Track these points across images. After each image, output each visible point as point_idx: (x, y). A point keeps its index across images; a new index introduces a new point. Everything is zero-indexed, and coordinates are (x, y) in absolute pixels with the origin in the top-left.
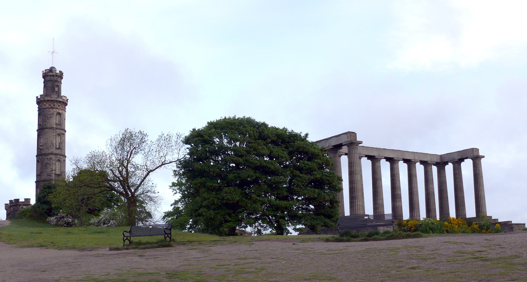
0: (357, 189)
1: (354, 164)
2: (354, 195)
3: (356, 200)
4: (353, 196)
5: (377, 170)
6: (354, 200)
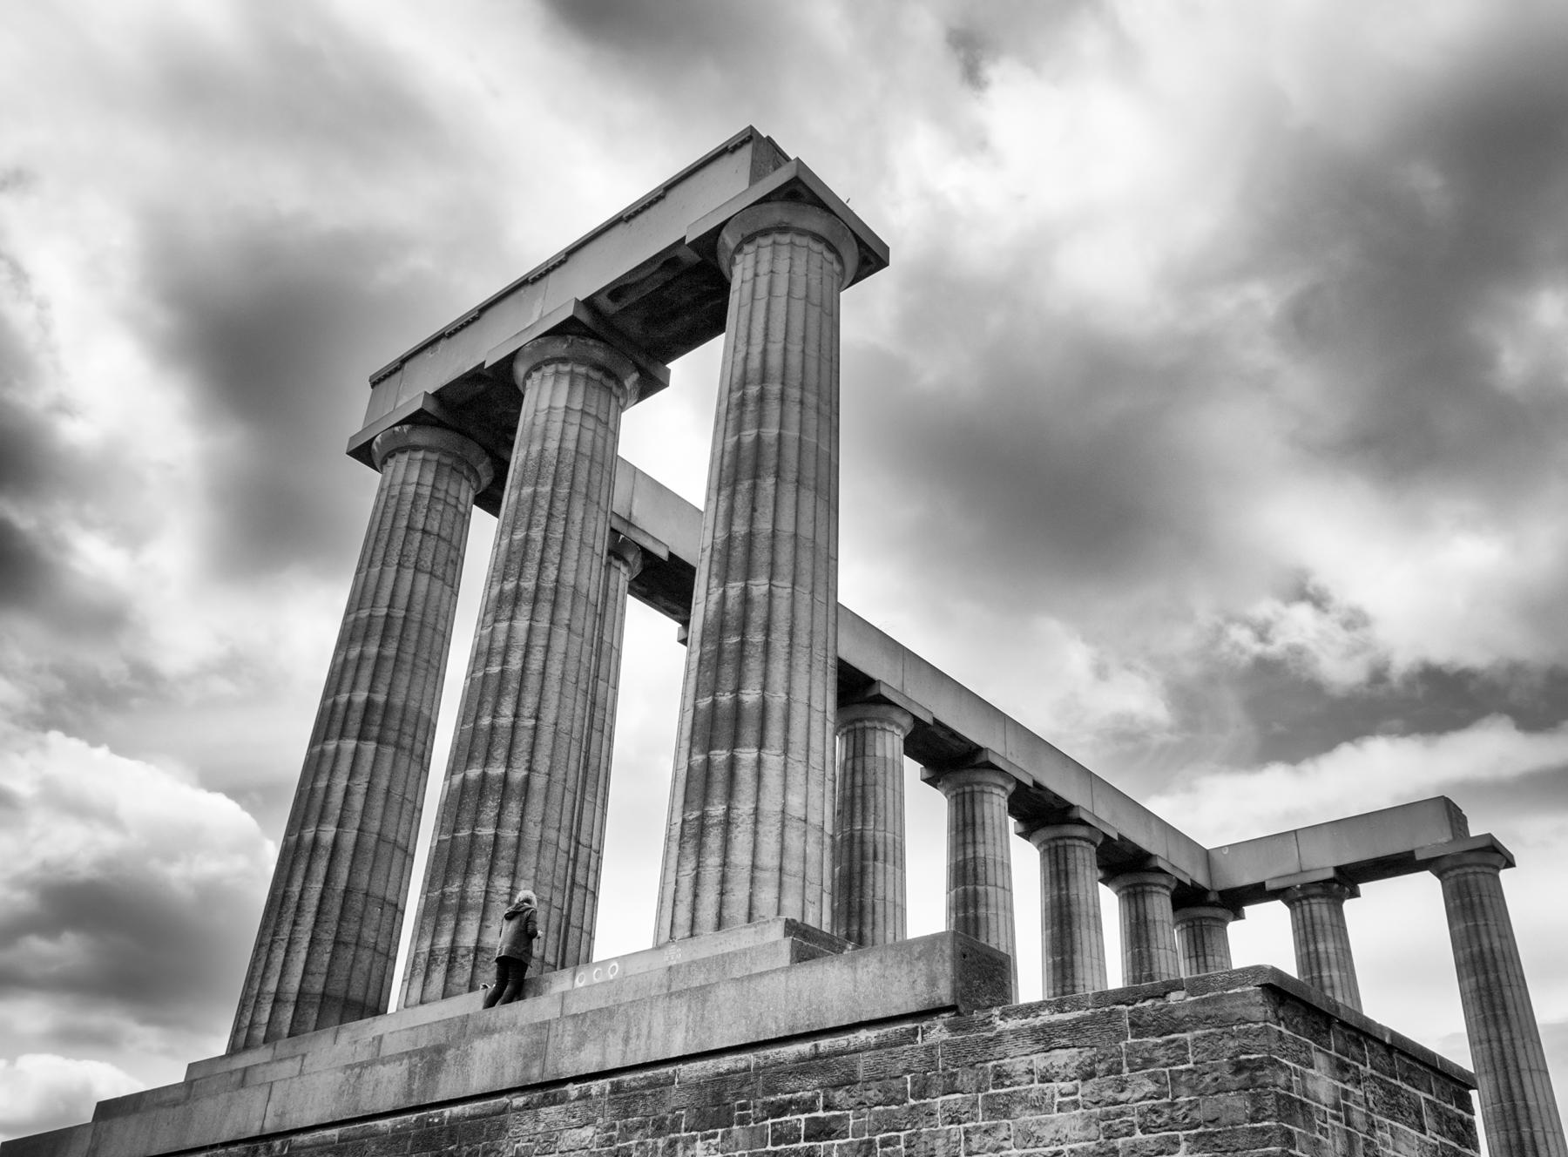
0: (792, 634)
1: (794, 393)
2: (750, 696)
3: (773, 759)
4: (738, 704)
5: (880, 790)
6: (747, 755)
